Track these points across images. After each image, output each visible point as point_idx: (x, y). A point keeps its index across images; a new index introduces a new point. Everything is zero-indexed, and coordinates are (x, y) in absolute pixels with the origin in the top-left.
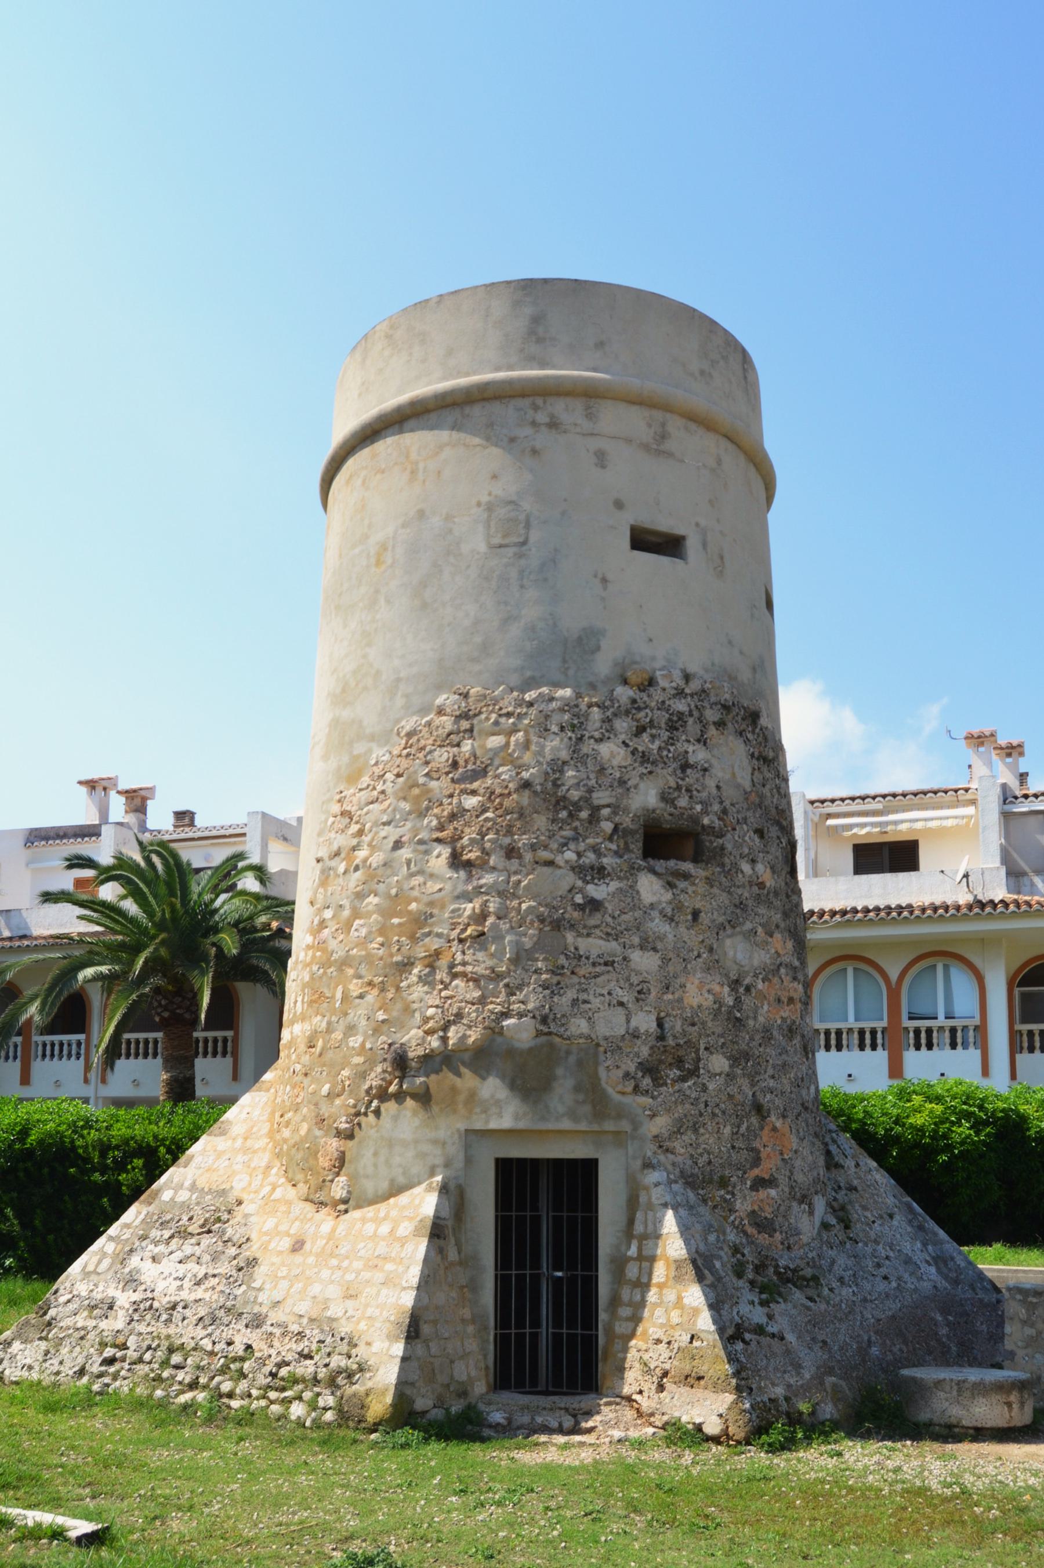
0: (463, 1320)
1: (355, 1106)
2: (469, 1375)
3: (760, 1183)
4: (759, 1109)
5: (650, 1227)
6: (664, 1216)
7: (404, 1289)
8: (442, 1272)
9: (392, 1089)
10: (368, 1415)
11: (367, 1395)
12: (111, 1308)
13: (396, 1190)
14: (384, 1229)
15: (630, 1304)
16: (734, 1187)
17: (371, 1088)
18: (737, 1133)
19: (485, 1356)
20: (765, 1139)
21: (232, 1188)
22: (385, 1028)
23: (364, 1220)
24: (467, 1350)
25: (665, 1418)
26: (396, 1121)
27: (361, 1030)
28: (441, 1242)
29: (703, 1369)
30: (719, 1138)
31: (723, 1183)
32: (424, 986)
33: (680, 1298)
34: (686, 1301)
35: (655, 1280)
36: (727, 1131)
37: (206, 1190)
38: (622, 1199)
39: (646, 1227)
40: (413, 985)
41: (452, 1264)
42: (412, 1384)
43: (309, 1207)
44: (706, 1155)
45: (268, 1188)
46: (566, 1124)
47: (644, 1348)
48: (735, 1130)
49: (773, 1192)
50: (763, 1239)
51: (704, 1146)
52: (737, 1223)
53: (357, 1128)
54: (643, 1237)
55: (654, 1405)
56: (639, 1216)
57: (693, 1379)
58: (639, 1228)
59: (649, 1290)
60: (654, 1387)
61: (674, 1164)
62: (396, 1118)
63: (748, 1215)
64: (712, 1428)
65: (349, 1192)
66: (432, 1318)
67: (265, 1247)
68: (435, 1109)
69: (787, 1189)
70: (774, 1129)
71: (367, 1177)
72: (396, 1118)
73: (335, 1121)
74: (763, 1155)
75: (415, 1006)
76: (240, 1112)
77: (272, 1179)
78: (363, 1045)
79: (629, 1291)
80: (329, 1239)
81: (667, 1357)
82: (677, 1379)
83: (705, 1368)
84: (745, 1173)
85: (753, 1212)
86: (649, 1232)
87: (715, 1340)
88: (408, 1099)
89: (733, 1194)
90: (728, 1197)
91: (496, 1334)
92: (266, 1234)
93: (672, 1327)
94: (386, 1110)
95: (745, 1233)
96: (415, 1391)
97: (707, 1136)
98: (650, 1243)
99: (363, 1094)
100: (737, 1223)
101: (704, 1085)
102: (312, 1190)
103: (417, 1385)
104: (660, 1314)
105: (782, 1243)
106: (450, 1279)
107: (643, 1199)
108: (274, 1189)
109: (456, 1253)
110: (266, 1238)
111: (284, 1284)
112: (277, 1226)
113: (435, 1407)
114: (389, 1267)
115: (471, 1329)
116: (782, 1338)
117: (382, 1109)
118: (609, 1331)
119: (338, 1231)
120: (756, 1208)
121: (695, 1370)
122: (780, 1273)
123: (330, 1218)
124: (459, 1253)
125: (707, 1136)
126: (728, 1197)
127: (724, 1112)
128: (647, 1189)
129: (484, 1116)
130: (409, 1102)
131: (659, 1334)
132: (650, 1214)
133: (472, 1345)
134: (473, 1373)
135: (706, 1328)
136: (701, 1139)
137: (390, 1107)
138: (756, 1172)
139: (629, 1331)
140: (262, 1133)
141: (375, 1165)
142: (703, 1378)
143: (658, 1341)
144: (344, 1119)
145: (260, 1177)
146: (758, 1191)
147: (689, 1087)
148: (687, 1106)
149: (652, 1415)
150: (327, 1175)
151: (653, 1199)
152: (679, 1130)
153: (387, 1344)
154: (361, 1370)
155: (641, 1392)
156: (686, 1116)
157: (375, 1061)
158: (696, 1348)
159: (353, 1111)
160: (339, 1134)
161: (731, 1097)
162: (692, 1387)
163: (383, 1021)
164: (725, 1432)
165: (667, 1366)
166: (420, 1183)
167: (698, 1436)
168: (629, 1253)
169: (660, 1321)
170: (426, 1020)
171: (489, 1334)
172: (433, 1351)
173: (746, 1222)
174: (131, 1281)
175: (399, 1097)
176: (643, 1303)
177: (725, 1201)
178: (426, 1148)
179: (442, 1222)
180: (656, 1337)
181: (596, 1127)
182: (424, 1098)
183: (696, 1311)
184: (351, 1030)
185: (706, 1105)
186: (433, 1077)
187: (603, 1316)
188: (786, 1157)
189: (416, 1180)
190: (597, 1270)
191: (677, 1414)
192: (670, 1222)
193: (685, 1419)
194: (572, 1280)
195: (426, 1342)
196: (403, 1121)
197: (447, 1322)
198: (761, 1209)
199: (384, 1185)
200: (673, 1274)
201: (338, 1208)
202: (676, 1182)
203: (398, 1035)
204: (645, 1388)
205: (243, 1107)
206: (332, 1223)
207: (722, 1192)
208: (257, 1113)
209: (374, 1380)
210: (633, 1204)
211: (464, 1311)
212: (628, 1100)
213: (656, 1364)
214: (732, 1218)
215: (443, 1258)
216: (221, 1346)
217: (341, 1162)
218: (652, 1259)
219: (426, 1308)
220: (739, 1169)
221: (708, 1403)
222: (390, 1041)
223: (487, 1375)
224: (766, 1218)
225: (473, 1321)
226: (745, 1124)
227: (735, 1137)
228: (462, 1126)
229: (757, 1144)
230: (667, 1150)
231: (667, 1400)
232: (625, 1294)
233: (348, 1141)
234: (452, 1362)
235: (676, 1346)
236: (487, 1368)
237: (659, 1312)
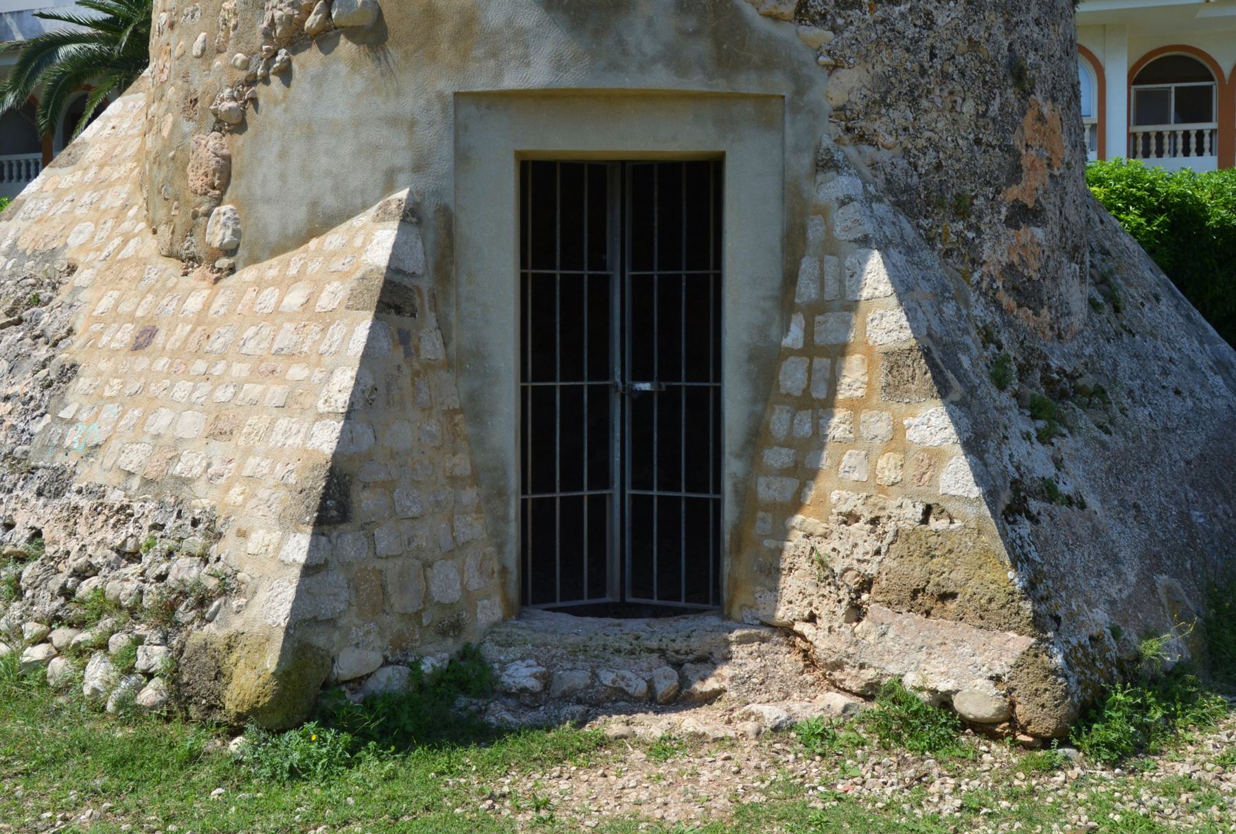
0: (453, 479)
1: (246, 65)
2: (464, 588)
3: (1022, 215)
4: (1018, 74)
5: (831, 288)
6: (862, 262)
7: (321, 416)
8: (406, 382)
9: (312, 21)
10: (228, 694)
11: (230, 648)
14: (295, 299)
15: (788, 443)
16: (980, 218)
18: (984, 115)
19: (500, 547)
20: (1028, 133)
21: (66, 245)
23: (260, 284)
24: (461, 539)
25: (869, 674)
28: (406, 322)
30: (955, 122)
31: (962, 209)
33: (898, 430)
34: (912, 435)
36: (969, 108)
37: (29, 252)
38: (773, 235)
41: (429, 366)
42: (331, 622)
43: (174, 266)
44: (931, 153)
45: (117, 241)
46: (660, 79)
47: (820, 531)
48: (982, 109)
49: (1039, 233)
50: (1024, 317)
51: (928, 134)
52: (984, 285)
54: (817, 308)
55: (841, 647)
56: (807, 266)
57: (929, 599)
58: (806, 290)
59: (832, 415)
60: (841, 610)
61: (874, 165)
62: (319, 80)
63: (1003, 272)
64: (978, 701)
65: (236, 233)
66: (382, 476)
67: (92, 344)
68: (395, 53)
69: (1057, 231)
70: (1041, 118)
72: (319, 80)
73: (213, 99)
74: (1025, 162)
76: (103, 128)
77: (126, 226)
79: (786, 417)
80: (198, 323)
82: (893, 597)
84: (998, 192)
85: (1011, 266)
87: (980, 518)
88: (343, 40)
89: (979, 231)
90: (971, 235)
91: (524, 502)
92: (98, 320)
93: (881, 489)
94: (302, 66)
95: (998, 304)
96: (336, 636)
97: (934, 114)
98: (832, 319)
99: (259, 39)
100: (984, 285)
101: (928, 14)
102: (178, 237)
103: (343, 622)
104: (853, 462)
105: (1052, 328)
106: (424, 396)
107: (815, 232)
108: (125, 243)
109: (439, 344)
110: (96, 327)
111: (110, 412)
112: (116, 305)
113: (386, 663)
114: (297, 372)
115: (470, 495)
116: (1083, 506)
118: (746, 495)
119: (215, 307)
120: (1016, 259)
121: (934, 579)
122: (1052, 381)
123: (205, 284)
124: (445, 344)
125: (934, 114)
126: (971, 235)
127: (962, 74)
128: (823, 212)
130: (345, 47)
132: (831, 262)
133: (473, 528)
134: (474, 583)
135: (960, 492)
136: (924, 120)
137: (308, 61)
138: (1013, 192)
139: (789, 495)
140: (127, 154)
141: (283, 177)
142: (953, 596)
143: (850, 518)
145: (110, 224)
146: (1018, 228)
147: (902, 15)
148: (899, 52)
149: (838, 666)
150: (200, 205)
151: (838, 232)
152: (883, 99)
153: (276, 535)
154: (225, 591)
155: (812, 619)
156: (896, 71)
158: (937, 533)
159: (242, 75)
161: (973, 44)
162: (928, 613)
164: (1009, 715)
165: (871, 569)
166: (365, 207)
168: (787, 342)
171: (507, 504)
172: (382, 546)
173: (1000, 284)
176: (818, 439)
177: (966, 242)
179: (407, 282)
180: (845, 508)
181: (720, 86)
183: (935, 458)
185: (933, 56)
187: (732, 467)
188: (1056, 173)
189: (358, 201)
190: (718, 376)
191: (893, 669)
192: (875, 276)
194: (669, 399)
195: (367, 528)
197: (415, 483)
198: (1024, 262)
199: (300, 215)
200: (881, 379)
201: (217, 264)
202: (880, 200)
204: (823, 612)
205: (109, 118)
206: (206, 293)
207: (960, 226)
208: (125, 125)
209: (246, 614)
210: (793, 243)
211: (456, 460)
212: (784, 32)
213: (847, 562)
214: (976, 276)
215: (408, 354)
218: (840, 351)
219: (369, 457)
220: (988, 183)
221: (967, 649)
223: (504, 585)
224: (1030, 279)
225: (475, 479)
226: (998, 99)
227: (981, 122)
228: (447, 86)
229: (1015, 141)
230: (862, 138)
231: (871, 638)
232: (779, 421)
233: (236, 136)
234: (428, 565)
235: (891, 527)
236: (504, 570)
237: (850, 458)
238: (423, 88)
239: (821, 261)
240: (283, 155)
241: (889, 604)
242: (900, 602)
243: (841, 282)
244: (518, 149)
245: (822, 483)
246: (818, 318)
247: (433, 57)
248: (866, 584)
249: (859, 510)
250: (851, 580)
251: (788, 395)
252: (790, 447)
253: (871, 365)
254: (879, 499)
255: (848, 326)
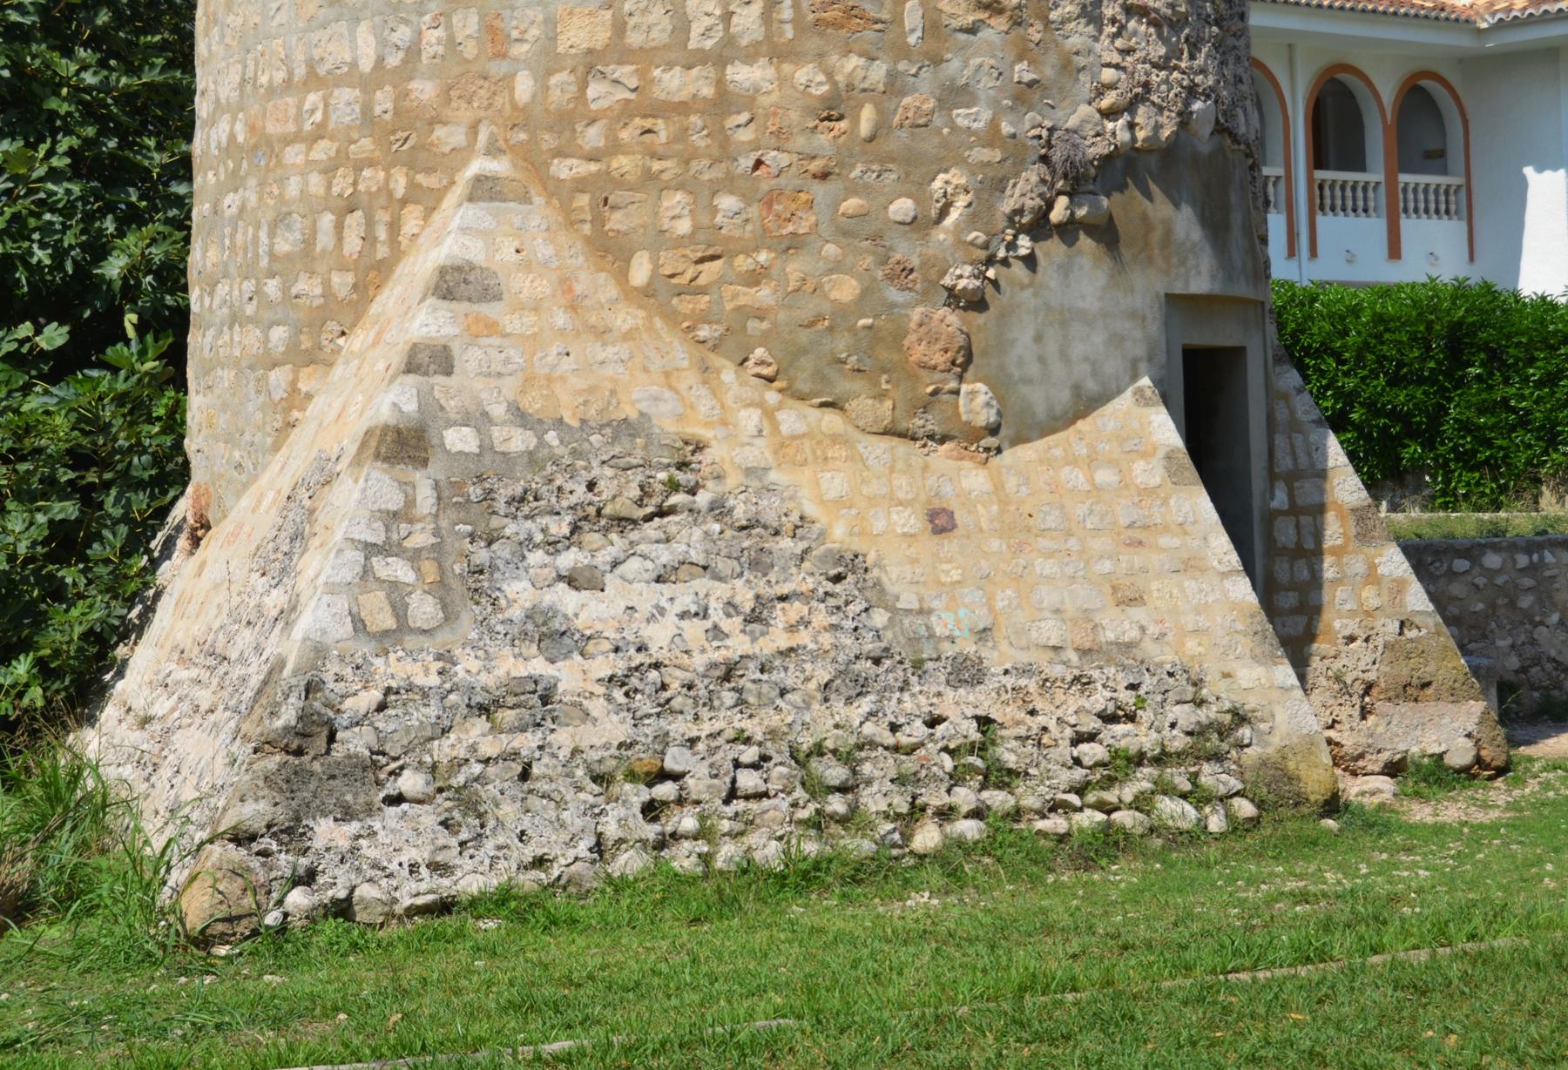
1: (986, 246)
5: (1303, 461)
6: (1325, 438)
9: (1058, 213)
12: (545, 700)
13: (1086, 404)
17: (1019, 212)
22: (1036, 96)
25: (1385, 756)
26: (1066, 275)
27: (982, 95)
29: (1427, 671)
32: (1088, 24)
33: (1373, 567)
35: (1328, 543)
39: (1295, 459)
40: (1069, 20)
47: (1333, 653)
53: (989, 289)
54: (1292, 478)
55: (1363, 740)
56: (1280, 440)
57: (1414, 690)
58: (1284, 463)
59: (1322, 561)
60: (1356, 713)
62: (1065, 270)
65: (999, 413)
68: (1126, 254)
71: (1028, 381)
72: (1065, 270)
73: (943, 273)
75: (1081, 61)
78: (994, 125)
79: (1286, 566)
81: (1370, 661)
82: (1391, 694)
83: (1431, 668)
86: (1302, 467)
87: (1437, 625)
88: (1082, 235)
93: (1368, 614)
94: (1047, 254)
98: (1307, 485)
104: (1344, 596)
107: (1281, 414)
117: (1038, 253)
121: (1416, 675)
129: (1183, 270)
130: (1085, 242)
131: (1352, 627)
132: (1298, 439)
135: (1421, 608)
139: (1301, 629)
141: (1042, 360)
142: (1429, 684)
143: (1351, 639)
144: (968, 270)
149: (1361, 756)
150: (945, 381)
151: (1299, 415)
157: (1023, 161)
158: (1412, 640)
159: (983, 254)
160: (953, 297)
162: (1416, 700)
163: (1031, 84)
164: (1478, 760)
165: (1371, 676)
166: (1119, 392)
167: (1435, 775)
168: (1275, 504)
169: (1348, 607)
170: (1102, 90)
174: (552, 635)
175: (1068, 231)
176: (1316, 582)
178: (1124, 326)
180: (1347, 633)
182: (1106, 233)
183: (1400, 586)
184: (956, 94)
186: (1116, 196)
189: (1114, 386)
191: (1402, 747)
192: (1335, 452)
193: (1415, 750)
196: (1079, 276)
199: (1063, 396)
200: (1353, 531)
201: (983, 443)
203: (1059, 114)
204: (1343, 717)
209: (1277, 732)
213: (1355, 674)
216: (918, 730)
217: (963, 362)
218: (1320, 509)
221: (1447, 720)
222: (1048, 124)
228: (1161, 287)
231: (1381, 729)
233: (972, 315)
235: (1380, 642)
238: (1147, 286)
239: (1290, 437)
240: (1038, 338)
241: (1389, 699)
242: (1397, 697)
243: (1309, 455)
244: (1187, 342)
245: (1327, 616)
246: (1296, 484)
247: (1150, 260)
248: (1369, 688)
249: (1357, 632)
250: (1359, 688)
251: (1285, 548)
252: (1294, 590)
253: (1342, 518)
254: (1368, 622)
255: (1322, 491)
